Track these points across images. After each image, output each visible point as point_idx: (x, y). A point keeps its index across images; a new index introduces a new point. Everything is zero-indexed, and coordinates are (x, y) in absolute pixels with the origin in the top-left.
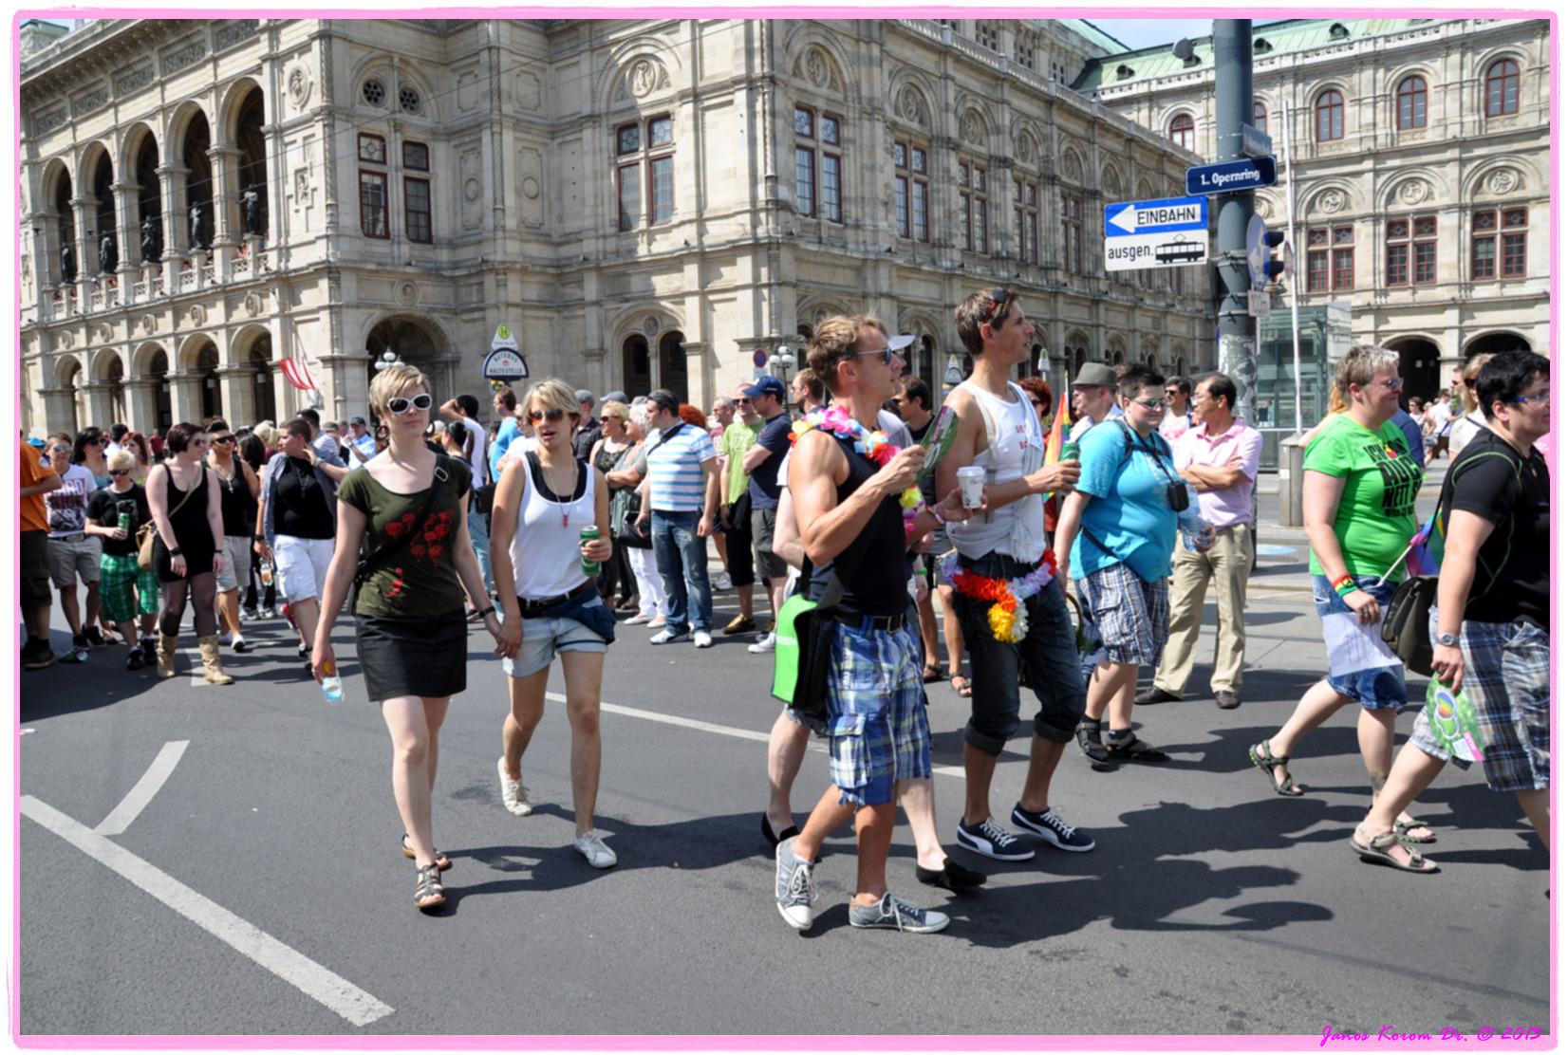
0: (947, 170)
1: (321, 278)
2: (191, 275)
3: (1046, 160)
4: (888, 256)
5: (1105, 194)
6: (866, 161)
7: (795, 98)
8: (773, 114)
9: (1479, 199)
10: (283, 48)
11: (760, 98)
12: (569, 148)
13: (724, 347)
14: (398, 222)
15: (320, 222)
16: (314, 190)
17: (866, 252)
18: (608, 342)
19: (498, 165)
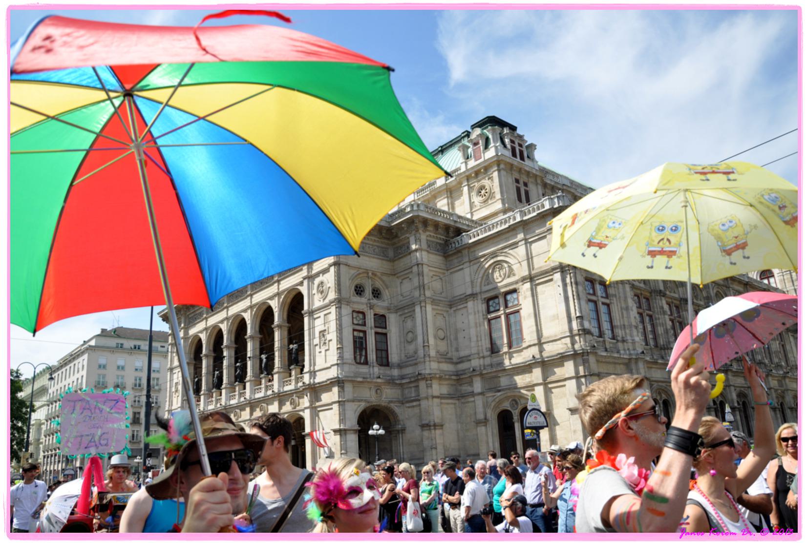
0: (662, 308)
1: (334, 386)
2: (260, 388)
4: (642, 356)
6: (623, 305)
8: (576, 283)
10: (314, 272)
11: (568, 276)
12: (460, 312)
13: (560, 412)
14: (372, 356)
15: (333, 357)
16: (330, 341)
17: (630, 354)
18: (489, 415)
19: (425, 323)
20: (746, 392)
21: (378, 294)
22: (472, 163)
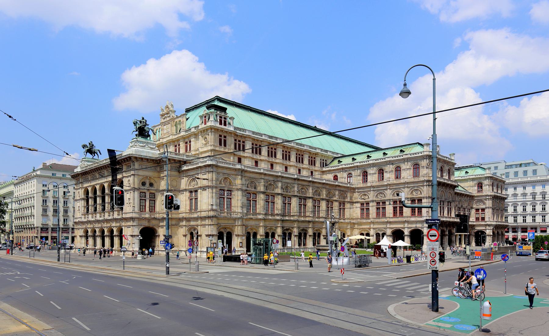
7: (220, 188)
13: (204, 236)
21: (152, 185)
22: (203, 126)
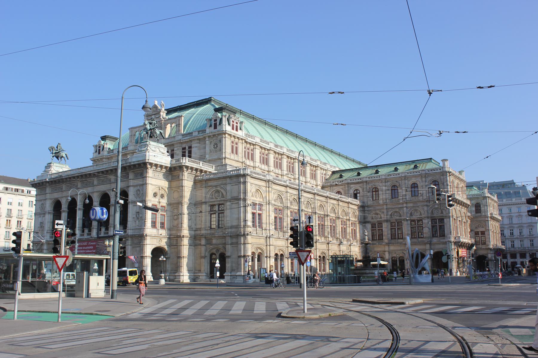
3: (314, 208)
5: (331, 215)
9: (433, 216)
14: (158, 225)
20: (326, 252)
